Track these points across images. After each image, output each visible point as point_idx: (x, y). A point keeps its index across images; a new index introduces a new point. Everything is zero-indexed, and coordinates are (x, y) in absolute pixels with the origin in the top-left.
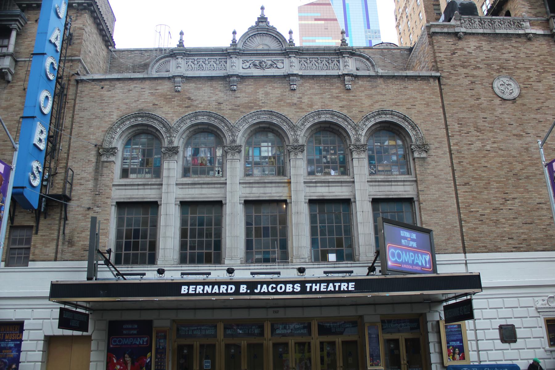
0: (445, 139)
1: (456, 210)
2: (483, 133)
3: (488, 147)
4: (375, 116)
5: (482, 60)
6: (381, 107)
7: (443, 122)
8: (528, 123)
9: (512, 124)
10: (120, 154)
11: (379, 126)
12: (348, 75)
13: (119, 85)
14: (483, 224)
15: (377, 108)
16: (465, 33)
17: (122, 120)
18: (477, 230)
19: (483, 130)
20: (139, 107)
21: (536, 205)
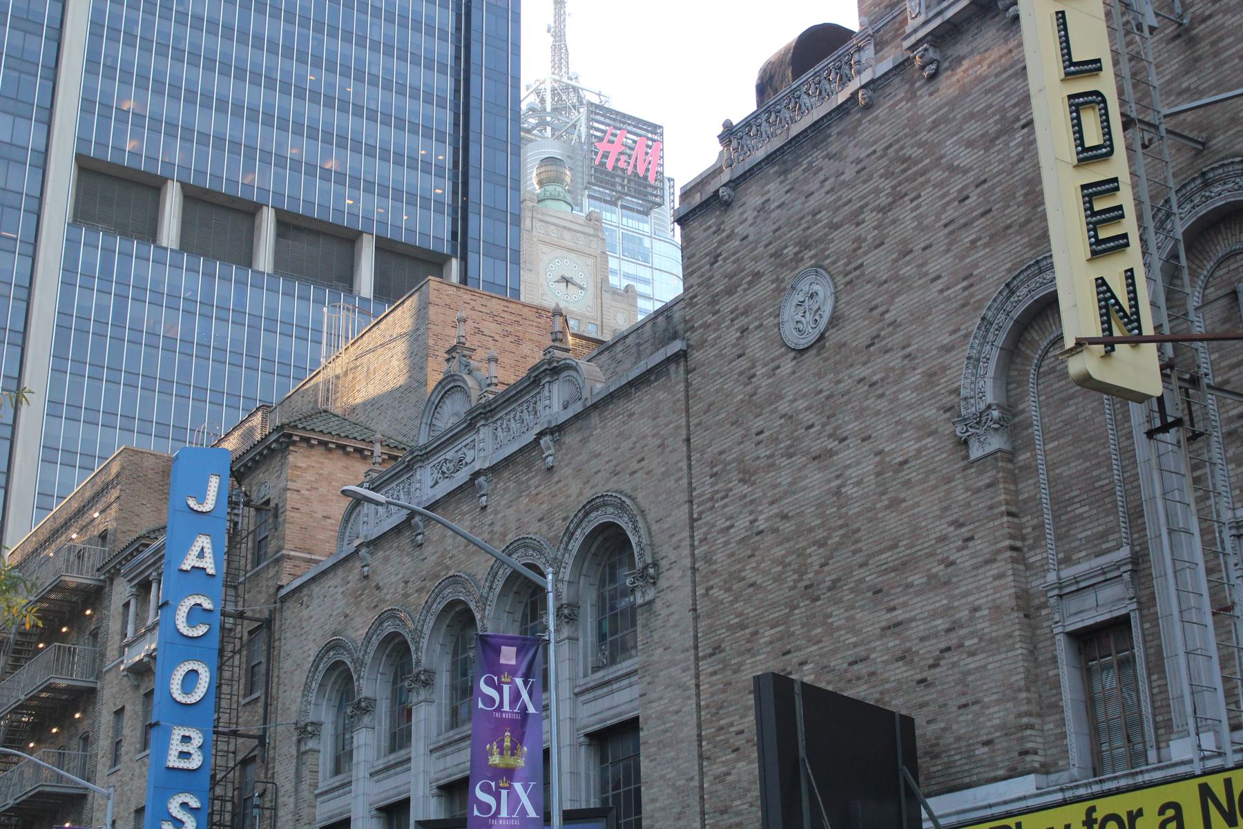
0: (686, 534)
1: (695, 732)
2: (754, 483)
3: (761, 524)
4: (581, 521)
5: (766, 246)
6: (593, 491)
7: (685, 482)
8: (846, 404)
9: (812, 426)
10: (328, 731)
11: (600, 538)
12: (541, 434)
13: (316, 589)
14: (738, 760)
15: (589, 494)
16: (730, 181)
17: (316, 665)
18: (729, 778)
19: (755, 472)
20: (333, 627)
21: (846, 671)
